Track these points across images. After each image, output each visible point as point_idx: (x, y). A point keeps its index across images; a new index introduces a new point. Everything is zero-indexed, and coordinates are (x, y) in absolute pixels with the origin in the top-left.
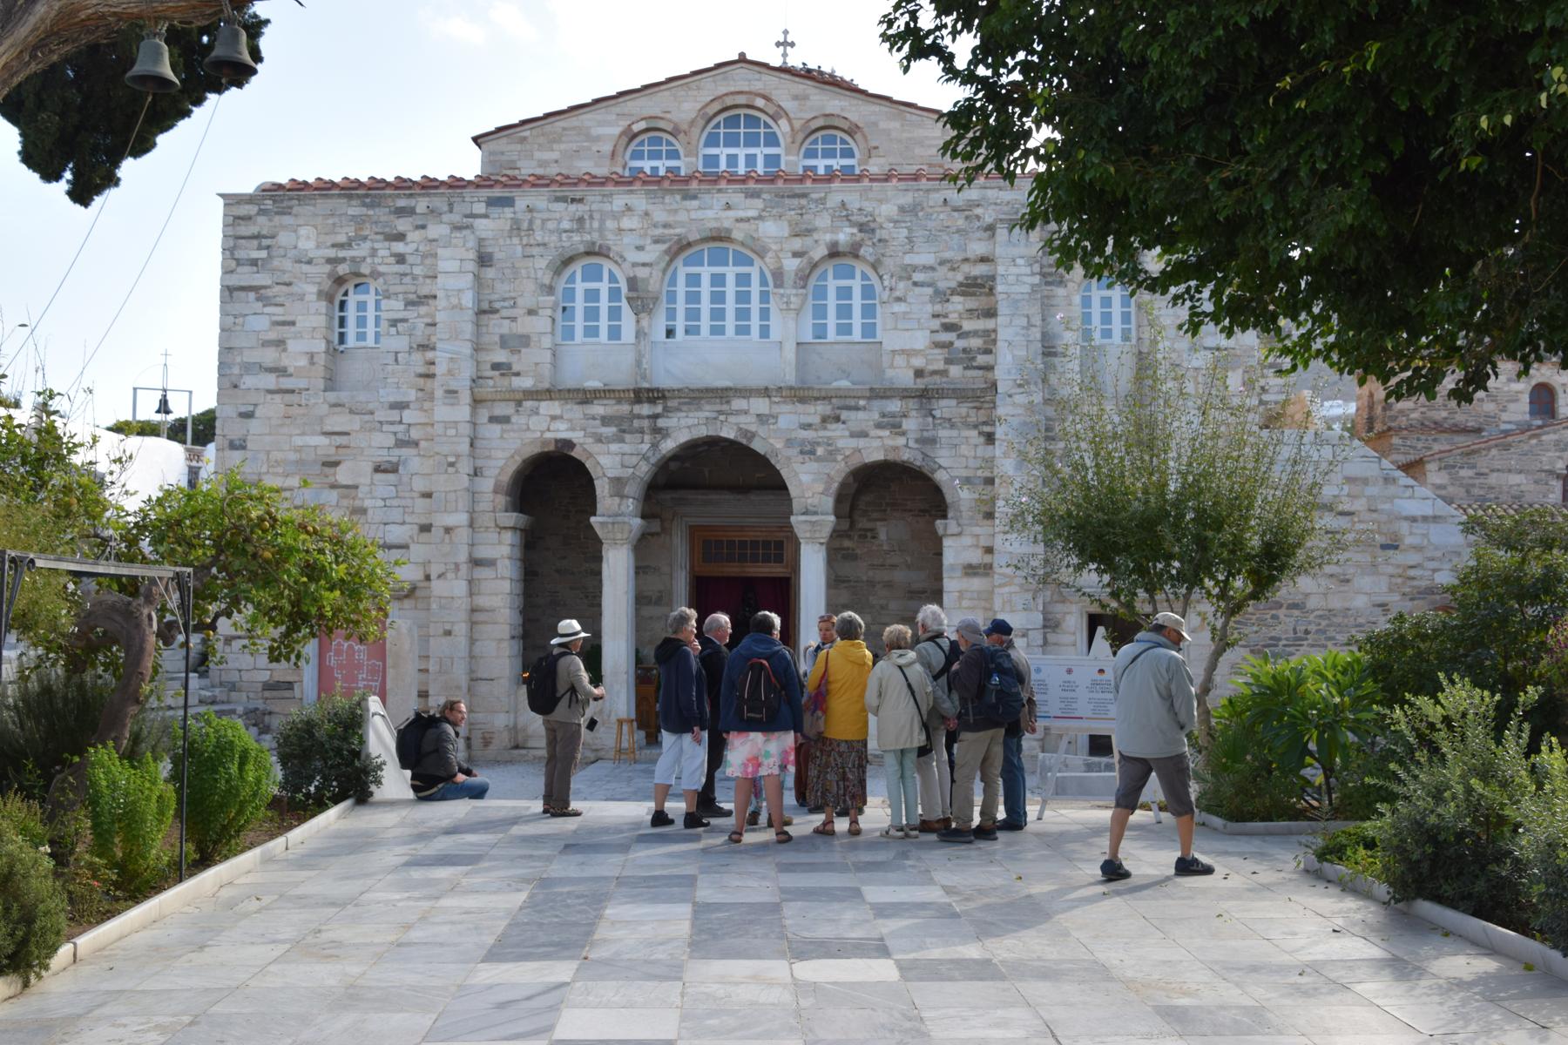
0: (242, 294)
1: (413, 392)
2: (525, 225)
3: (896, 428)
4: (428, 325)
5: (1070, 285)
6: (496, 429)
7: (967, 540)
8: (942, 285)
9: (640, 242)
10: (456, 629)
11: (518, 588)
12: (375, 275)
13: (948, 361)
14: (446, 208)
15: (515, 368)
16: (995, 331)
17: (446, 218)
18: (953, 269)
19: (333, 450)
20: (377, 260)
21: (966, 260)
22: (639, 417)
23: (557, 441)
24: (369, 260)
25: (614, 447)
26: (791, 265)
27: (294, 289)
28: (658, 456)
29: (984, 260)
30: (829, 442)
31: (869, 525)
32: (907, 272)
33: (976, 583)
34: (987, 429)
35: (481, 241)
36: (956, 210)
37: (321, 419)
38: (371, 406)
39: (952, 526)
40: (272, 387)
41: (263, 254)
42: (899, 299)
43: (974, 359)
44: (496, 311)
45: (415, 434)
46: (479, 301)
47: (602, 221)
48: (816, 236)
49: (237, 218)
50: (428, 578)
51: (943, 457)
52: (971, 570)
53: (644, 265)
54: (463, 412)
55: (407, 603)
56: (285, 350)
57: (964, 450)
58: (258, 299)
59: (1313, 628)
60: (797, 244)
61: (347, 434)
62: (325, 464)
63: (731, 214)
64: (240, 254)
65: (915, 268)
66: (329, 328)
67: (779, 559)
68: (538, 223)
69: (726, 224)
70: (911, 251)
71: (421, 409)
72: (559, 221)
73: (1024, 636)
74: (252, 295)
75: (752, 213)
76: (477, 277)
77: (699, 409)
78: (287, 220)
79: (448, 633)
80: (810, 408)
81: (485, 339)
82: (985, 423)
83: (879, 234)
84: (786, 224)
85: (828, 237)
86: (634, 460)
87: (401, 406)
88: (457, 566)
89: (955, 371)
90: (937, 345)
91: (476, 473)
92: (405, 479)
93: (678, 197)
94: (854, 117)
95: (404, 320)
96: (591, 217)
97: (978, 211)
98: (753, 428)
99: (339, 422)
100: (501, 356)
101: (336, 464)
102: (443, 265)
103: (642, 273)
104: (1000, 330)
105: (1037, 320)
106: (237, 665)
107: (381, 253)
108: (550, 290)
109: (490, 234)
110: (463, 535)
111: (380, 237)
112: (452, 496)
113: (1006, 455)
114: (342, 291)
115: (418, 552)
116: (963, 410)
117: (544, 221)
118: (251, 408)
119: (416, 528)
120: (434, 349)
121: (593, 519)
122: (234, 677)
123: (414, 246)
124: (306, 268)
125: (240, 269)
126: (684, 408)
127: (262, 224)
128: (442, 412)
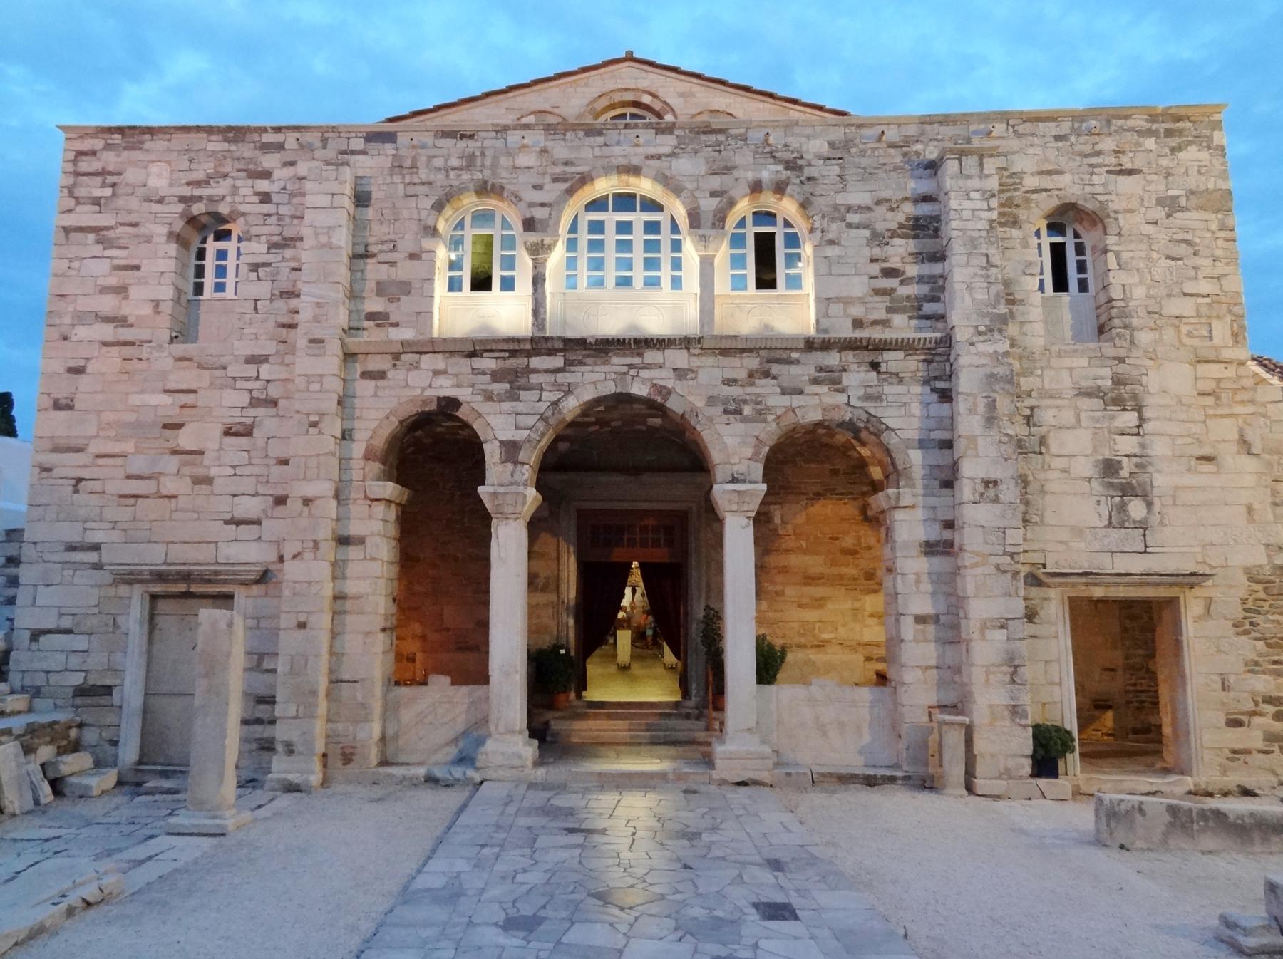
0: (80, 235)
2: (408, 163)
5: (1026, 226)
6: (371, 384)
8: (880, 227)
9: (538, 181)
10: (312, 620)
11: (394, 571)
14: (319, 144)
15: (393, 319)
17: (320, 154)
18: (892, 210)
19: (177, 410)
20: (237, 199)
22: (535, 371)
23: (439, 398)
24: (228, 199)
25: (506, 406)
27: (141, 230)
29: (926, 199)
32: (838, 213)
37: (164, 375)
38: (224, 360)
40: (110, 339)
41: (108, 192)
42: (832, 242)
43: (920, 308)
44: (374, 255)
45: (274, 391)
46: (354, 244)
47: (495, 158)
48: (736, 173)
49: (80, 153)
50: (281, 559)
52: (930, 548)
53: (543, 205)
54: (331, 362)
55: (256, 590)
56: (126, 298)
58: (98, 242)
60: (715, 183)
61: (194, 391)
62: (165, 426)
63: (640, 150)
64: (81, 192)
65: (849, 209)
66: (181, 273)
68: (422, 160)
70: (843, 190)
71: (282, 363)
73: (1002, 627)
74: (91, 237)
75: (667, 150)
77: (606, 362)
79: (302, 625)
80: (735, 361)
82: (936, 378)
83: (808, 172)
85: (750, 175)
86: (531, 420)
89: (899, 320)
90: (877, 292)
91: (346, 435)
93: (581, 134)
95: (269, 265)
96: (483, 154)
98: (669, 384)
99: (186, 377)
101: (179, 426)
106: (45, 666)
107: (243, 191)
109: (368, 173)
111: (243, 174)
113: (972, 411)
115: (271, 528)
117: (430, 158)
118: (82, 363)
119: (271, 499)
120: (298, 296)
121: (480, 489)
122: (40, 680)
123: (282, 184)
124: (156, 208)
125: (79, 208)
126: (589, 361)
127: (109, 160)
128: (304, 363)
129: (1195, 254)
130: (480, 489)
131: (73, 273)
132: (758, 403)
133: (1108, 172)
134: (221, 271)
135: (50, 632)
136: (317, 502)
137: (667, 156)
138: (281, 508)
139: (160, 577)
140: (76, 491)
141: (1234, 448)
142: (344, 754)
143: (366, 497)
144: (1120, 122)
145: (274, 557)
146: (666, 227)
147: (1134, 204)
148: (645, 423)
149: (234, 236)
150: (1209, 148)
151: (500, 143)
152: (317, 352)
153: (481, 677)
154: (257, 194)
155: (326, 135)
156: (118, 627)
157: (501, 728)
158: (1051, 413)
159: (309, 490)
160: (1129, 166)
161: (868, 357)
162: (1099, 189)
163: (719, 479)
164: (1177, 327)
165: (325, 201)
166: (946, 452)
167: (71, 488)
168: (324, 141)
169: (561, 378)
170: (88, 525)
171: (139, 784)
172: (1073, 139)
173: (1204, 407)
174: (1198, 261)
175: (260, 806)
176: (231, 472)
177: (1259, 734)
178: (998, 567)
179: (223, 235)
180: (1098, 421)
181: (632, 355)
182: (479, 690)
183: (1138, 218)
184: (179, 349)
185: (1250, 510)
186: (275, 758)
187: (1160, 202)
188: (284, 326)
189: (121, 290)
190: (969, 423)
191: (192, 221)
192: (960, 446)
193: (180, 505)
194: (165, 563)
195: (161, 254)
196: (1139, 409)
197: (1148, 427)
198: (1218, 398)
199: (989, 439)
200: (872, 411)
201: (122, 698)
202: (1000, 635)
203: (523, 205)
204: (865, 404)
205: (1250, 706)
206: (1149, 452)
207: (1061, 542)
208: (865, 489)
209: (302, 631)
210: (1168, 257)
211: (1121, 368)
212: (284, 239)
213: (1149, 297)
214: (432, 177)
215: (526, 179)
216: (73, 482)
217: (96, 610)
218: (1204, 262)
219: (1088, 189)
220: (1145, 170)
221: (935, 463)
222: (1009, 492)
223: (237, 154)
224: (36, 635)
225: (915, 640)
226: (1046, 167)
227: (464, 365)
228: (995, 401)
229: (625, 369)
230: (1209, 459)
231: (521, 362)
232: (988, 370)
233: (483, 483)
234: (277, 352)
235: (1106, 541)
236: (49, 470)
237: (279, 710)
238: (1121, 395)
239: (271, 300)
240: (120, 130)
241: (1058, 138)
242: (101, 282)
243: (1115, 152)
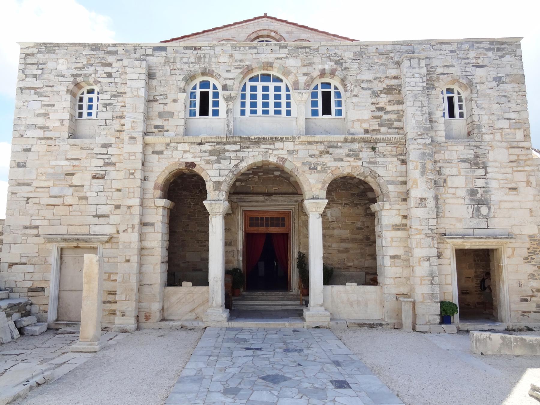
0: (27, 91)
1: (114, 139)
2: (172, 60)
4: (122, 106)
5: (438, 89)
6: (156, 157)
7: (394, 212)
8: (375, 89)
9: (229, 69)
10: (132, 258)
11: (166, 237)
12: (96, 82)
13: (380, 125)
14: (133, 52)
19: (71, 168)
20: (97, 75)
22: (228, 151)
23: (186, 163)
24: (93, 75)
25: (215, 166)
26: (302, 80)
27: (55, 89)
28: (238, 171)
29: (396, 77)
30: (324, 164)
32: (358, 83)
33: (400, 234)
34: (402, 157)
35: (150, 67)
36: (381, 54)
38: (91, 146)
39: (387, 206)
40: (41, 136)
41: (40, 72)
42: (355, 96)
45: (114, 160)
46: (148, 96)
47: (210, 58)
48: (314, 66)
49: (27, 55)
50: (118, 232)
51: (381, 171)
52: (396, 227)
53: (230, 79)
54: (139, 148)
55: (108, 245)
56: (49, 118)
57: (391, 167)
58: (35, 94)
60: (305, 70)
61: (79, 159)
62: (66, 175)
63: (274, 56)
64: (27, 72)
65: (363, 81)
66: (72, 108)
67: (283, 225)
68: (178, 60)
69: (270, 60)
71: (117, 148)
72: (189, 58)
73: (428, 260)
74: (33, 92)
75: (284, 56)
77: (259, 147)
78: (52, 56)
79: (128, 261)
80: (314, 147)
81: (151, 114)
82: (400, 155)
84: (300, 60)
85: (320, 67)
86: (226, 172)
87: (107, 146)
88: (133, 226)
89: (384, 129)
91: (145, 179)
92: (108, 182)
93: (247, 48)
95: (111, 104)
96: (205, 56)
97: (392, 55)
99: (76, 153)
100: (159, 122)
101: (73, 174)
103: (229, 83)
105: (426, 103)
106: (14, 279)
107: (99, 72)
108: (184, 91)
110: (136, 210)
111: (100, 65)
112: (132, 190)
113: (415, 169)
114: (81, 92)
115: (115, 219)
116: (389, 148)
118: (29, 147)
119: (113, 206)
120: (124, 118)
121: (205, 202)
122: (13, 285)
124: (61, 79)
125: (27, 79)
126: (251, 146)
127: (40, 57)
128: (127, 148)
129: (509, 101)
130: (205, 202)
131: (25, 107)
132: (324, 165)
133: (473, 66)
134: (90, 107)
135: (17, 264)
136: (133, 208)
137: (284, 58)
138: (118, 210)
139: (65, 240)
140: (27, 203)
141: (524, 184)
142: (146, 316)
143: (155, 205)
144: (478, 45)
145: (115, 232)
146: (283, 89)
147: (484, 80)
148: (273, 174)
149: (96, 92)
151: (212, 52)
152: (133, 142)
153: (205, 282)
154: (105, 73)
155: (136, 48)
156: (47, 262)
157: (214, 305)
158: (448, 169)
159: (130, 202)
160: (481, 64)
161: (371, 145)
162: (469, 74)
163: (307, 198)
164: (501, 133)
165: (136, 76)
166: (404, 186)
167: (25, 202)
168: (135, 50)
169: (239, 154)
170: (32, 218)
171: (57, 330)
172: (458, 52)
173: (512, 167)
174: (510, 105)
175: (111, 339)
176: (96, 194)
177: (534, 305)
178: (426, 235)
179: (91, 92)
180: (468, 172)
182: (204, 288)
184: (72, 141)
185: (531, 211)
186: (116, 318)
187: (495, 79)
188: (118, 131)
189: (46, 115)
190: (415, 174)
191: (77, 85)
192: (410, 183)
193: (74, 209)
194: (67, 234)
195: (63, 99)
196: (485, 168)
197: (489, 176)
198: (519, 163)
199: (422, 180)
200: (373, 169)
201: (49, 292)
202: (427, 263)
203: (221, 79)
204: (369, 166)
205: (531, 293)
206: (489, 186)
207: (452, 224)
208: (367, 202)
209: (127, 263)
210: (497, 103)
211: (478, 151)
212: (118, 93)
213: (490, 120)
214: (182, 67)
215: (223, 68)
216: (26, 199)
217: (37, 255)
219: (464, 73)
220: (488, 65)
221: (399, 191)
222: (431, 203)
223: (97, 56)
224: (11, 265)
225: (391, 266)
226: (446, 64)
227: (198, 148)
228: (425, 164)
229: (267, 150)
230: (514, 189)
231: (222, 147)
232: (422, 151)
233: (205, 199)
234: (116, 142)
235: (471, 224)
236: (16, 193)
237: (118, 297)
238: (478, 162)
240: (45, 44)
241: (452, 51)
243: (476, 57)
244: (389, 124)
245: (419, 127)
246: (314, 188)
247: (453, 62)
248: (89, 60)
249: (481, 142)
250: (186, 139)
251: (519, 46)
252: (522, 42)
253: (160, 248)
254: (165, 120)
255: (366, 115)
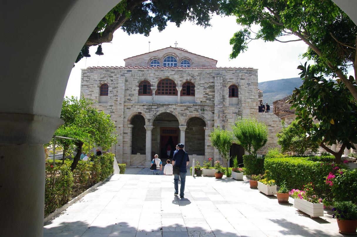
0: (84, 86)
2: (133, 75)
3: (197, 111)
6: (128, 110)
8: (205, 87)
10: (121, 144)
11: (131, 138)
14: (120, 72)
16: (214, 95)
18: (207, 84)
21: (209, 82)
22: (153, 108)
23: (138, 112)
24: (106, 81)
26: (179, 83)
29: (213, 82)
31: (192, 128)
32: (199, 84)
34: (213, 111)
41: (88, 79)
42: (198, 89)
44: (128, 90)
45: (114, 111)
46: (125, 88)
48: (184, 78)
49: (84, 73)
51: (205, 116)
53: (154, 82)
54: (122, 107)
56: (92, 96)
57: (209, 115)
58: (87, 87)
59: (267, 146)
60: (181, 79)
63: (169, 74)
64: (84, 79)
65: (201, 84)
69: (168, 75)
72: (140, 74)
74: (86, 86)
75: (173, 74)
76: (125, 84)
77: (163, 107)
78: (92, 73)
79: (119, 145)
80: (183, 107)
82: (213, 110)
83: (195, 78)
85: (186, 78)
86: (152, 116)
87: (111, 106)
89: (208, 101)
90: (204, 97)
91: (124, 118)
93: (160, 71)
94: (190, 57)
97: (212, 74)
100: (129, 98)
102: (119, 82)
103: (154, 83)
104: (215, 95)
105: (222, 93)
107: (109, 79)
110: (122, 128)
113: (216, 116)
121: (145, 126)
124: (96, 82)
125: (84, 82)
128: (119, 107)
147: (244, 84)
150: (255, 76)
153: (145, 154)
154: (110, 80)
157: (148, 160)
159: (120, 126)
160: (243, 78)
162: (238, 82)
165: (121, 82)
166: (213, 121)
172: (235, 74)
174: (252, 93)
181: (167, 106)
183: (243, 87)
184: (100, 104)
187: (247, 84)
188: (115, 101)
189: (91, 95)
190: (216, 118)
210: (248, 93)
211: (239, 110)
214: (137, 78)
215: (152, 78)
218: (253, 94)
221: (211, 123)
225: (207, 149)
226: (230, 78)
227: (142, 107)
231: (150, 107)
234: (114, 105)
239: (113, 97)
241: (233, 73)
242: (88, 94)
244: (209, 99)
245: (219, 101)
246: (182, 121)
247: (233, 77)
248: (105, 75)
249: (241, 107)
250: (138, 104)
251: (257, 72)
252: (258, 71)
253: (129, 142)
254: (131, 97)
255: (202, 96)
